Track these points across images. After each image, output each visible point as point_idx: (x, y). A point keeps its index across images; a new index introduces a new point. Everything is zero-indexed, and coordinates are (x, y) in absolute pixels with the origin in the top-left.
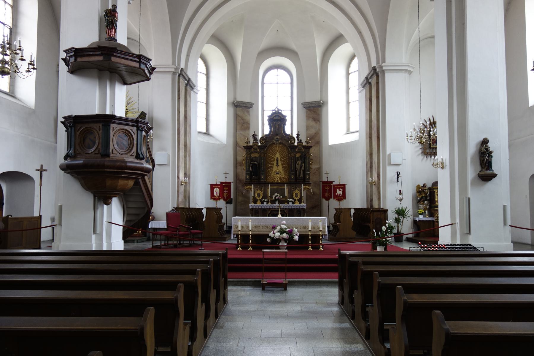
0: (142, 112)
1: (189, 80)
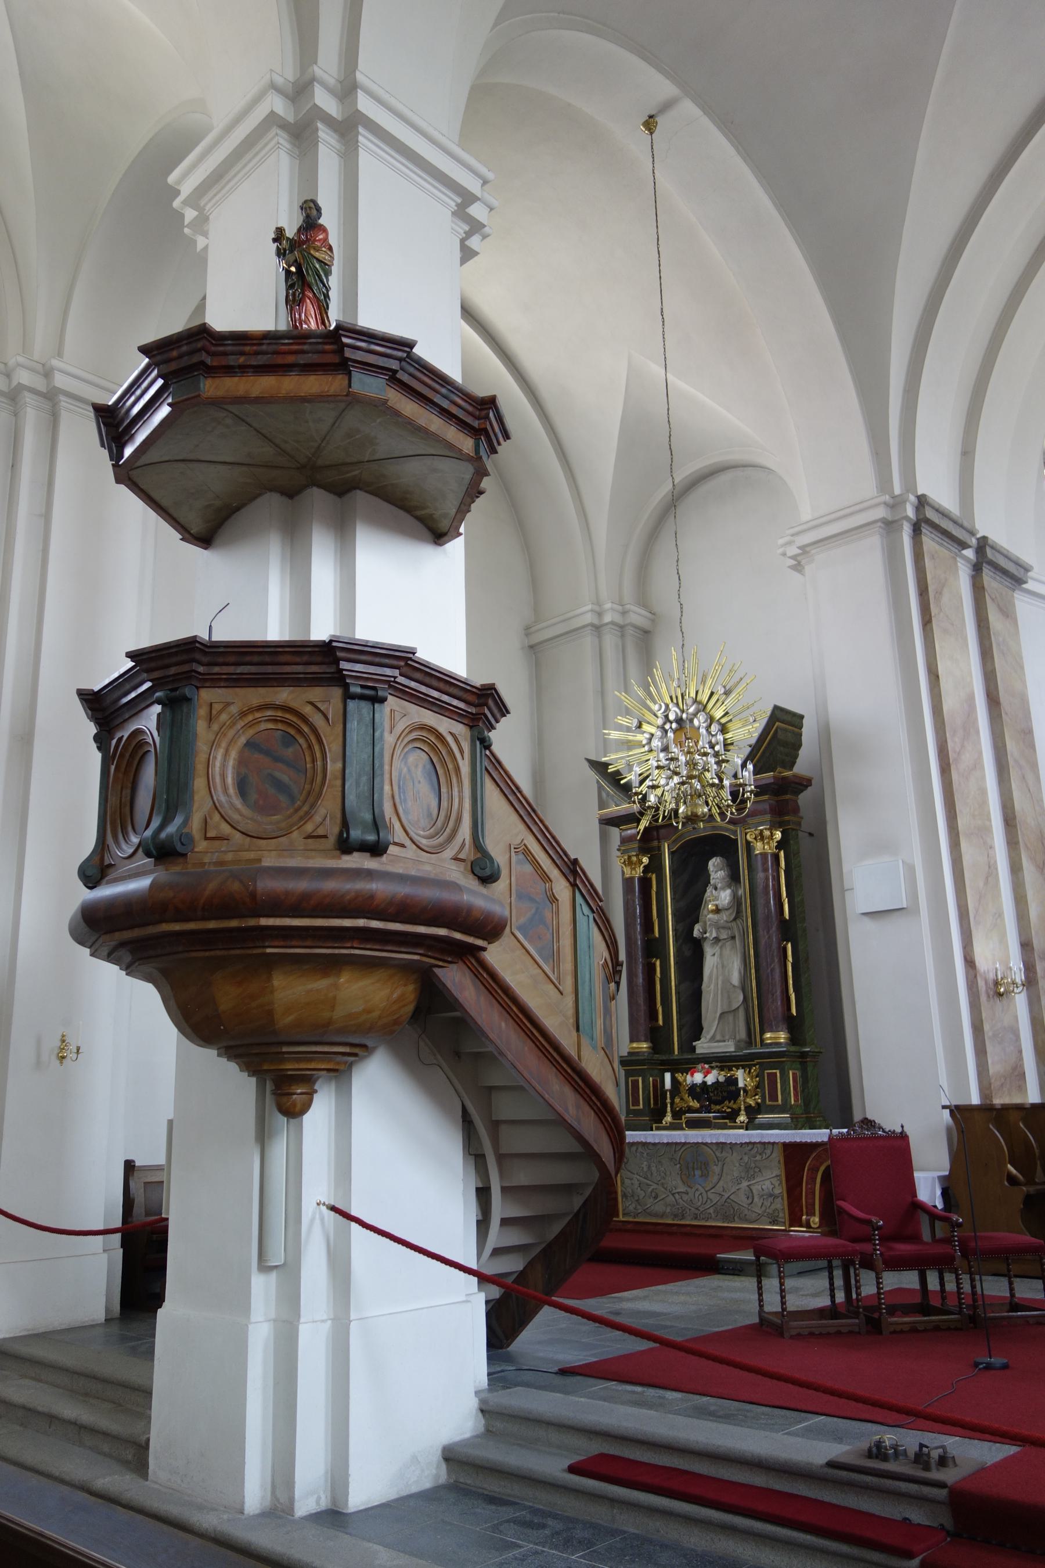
0: (776, 708)
1: (983, 545)
